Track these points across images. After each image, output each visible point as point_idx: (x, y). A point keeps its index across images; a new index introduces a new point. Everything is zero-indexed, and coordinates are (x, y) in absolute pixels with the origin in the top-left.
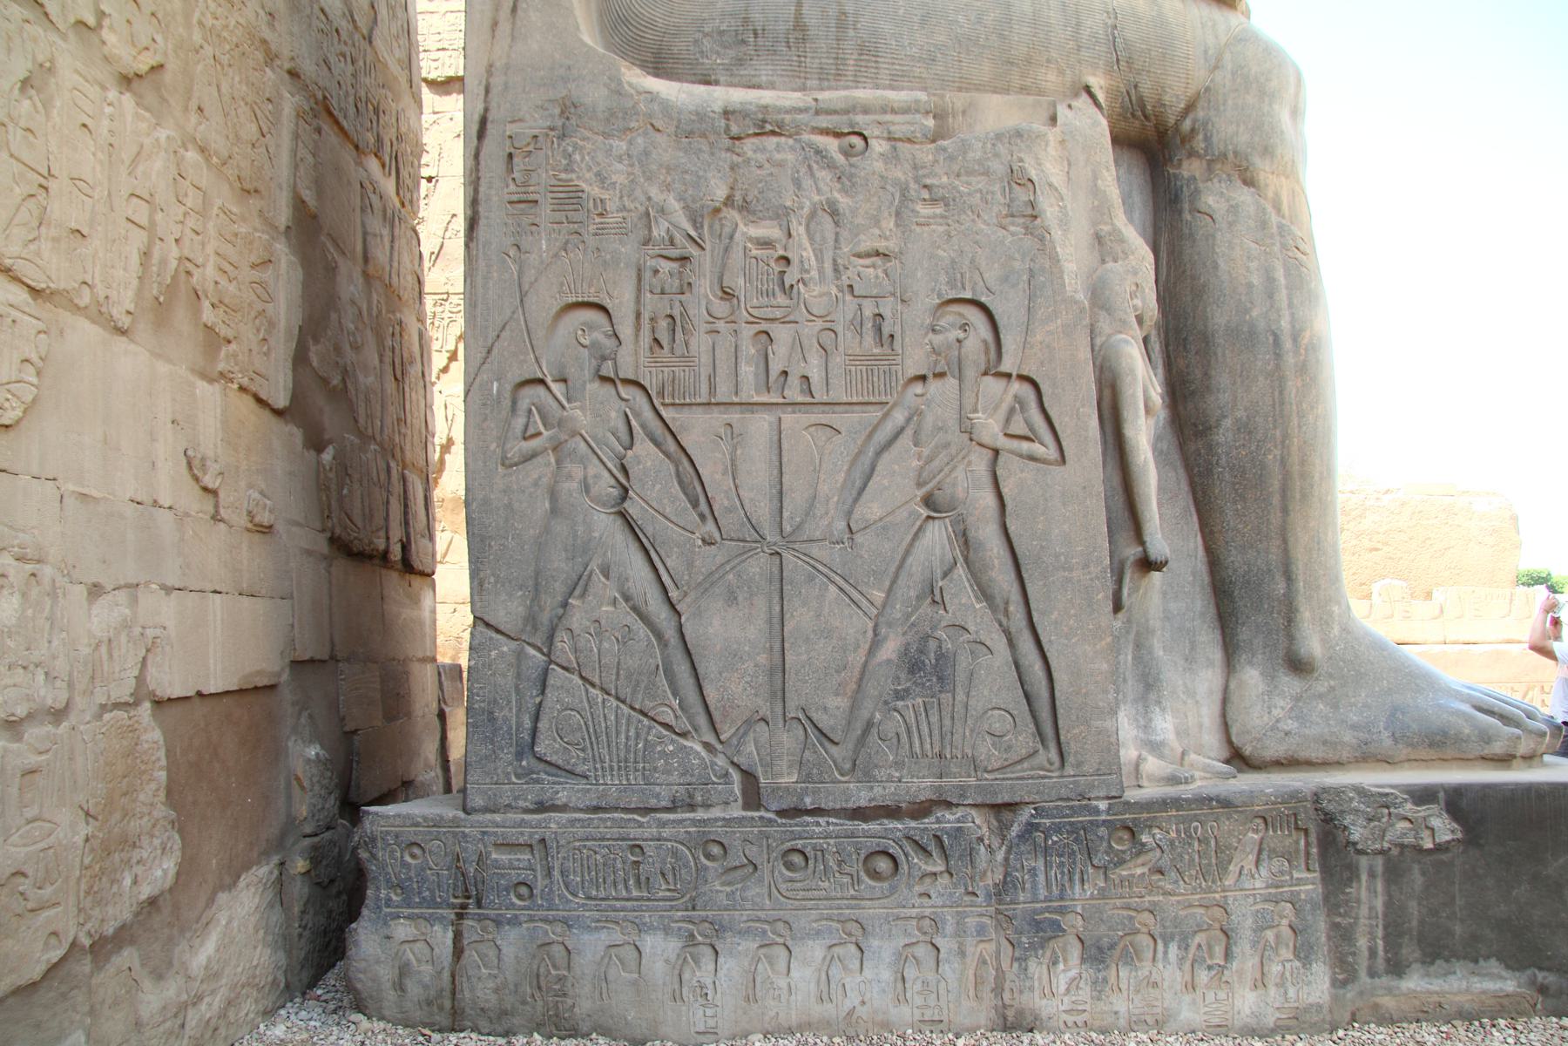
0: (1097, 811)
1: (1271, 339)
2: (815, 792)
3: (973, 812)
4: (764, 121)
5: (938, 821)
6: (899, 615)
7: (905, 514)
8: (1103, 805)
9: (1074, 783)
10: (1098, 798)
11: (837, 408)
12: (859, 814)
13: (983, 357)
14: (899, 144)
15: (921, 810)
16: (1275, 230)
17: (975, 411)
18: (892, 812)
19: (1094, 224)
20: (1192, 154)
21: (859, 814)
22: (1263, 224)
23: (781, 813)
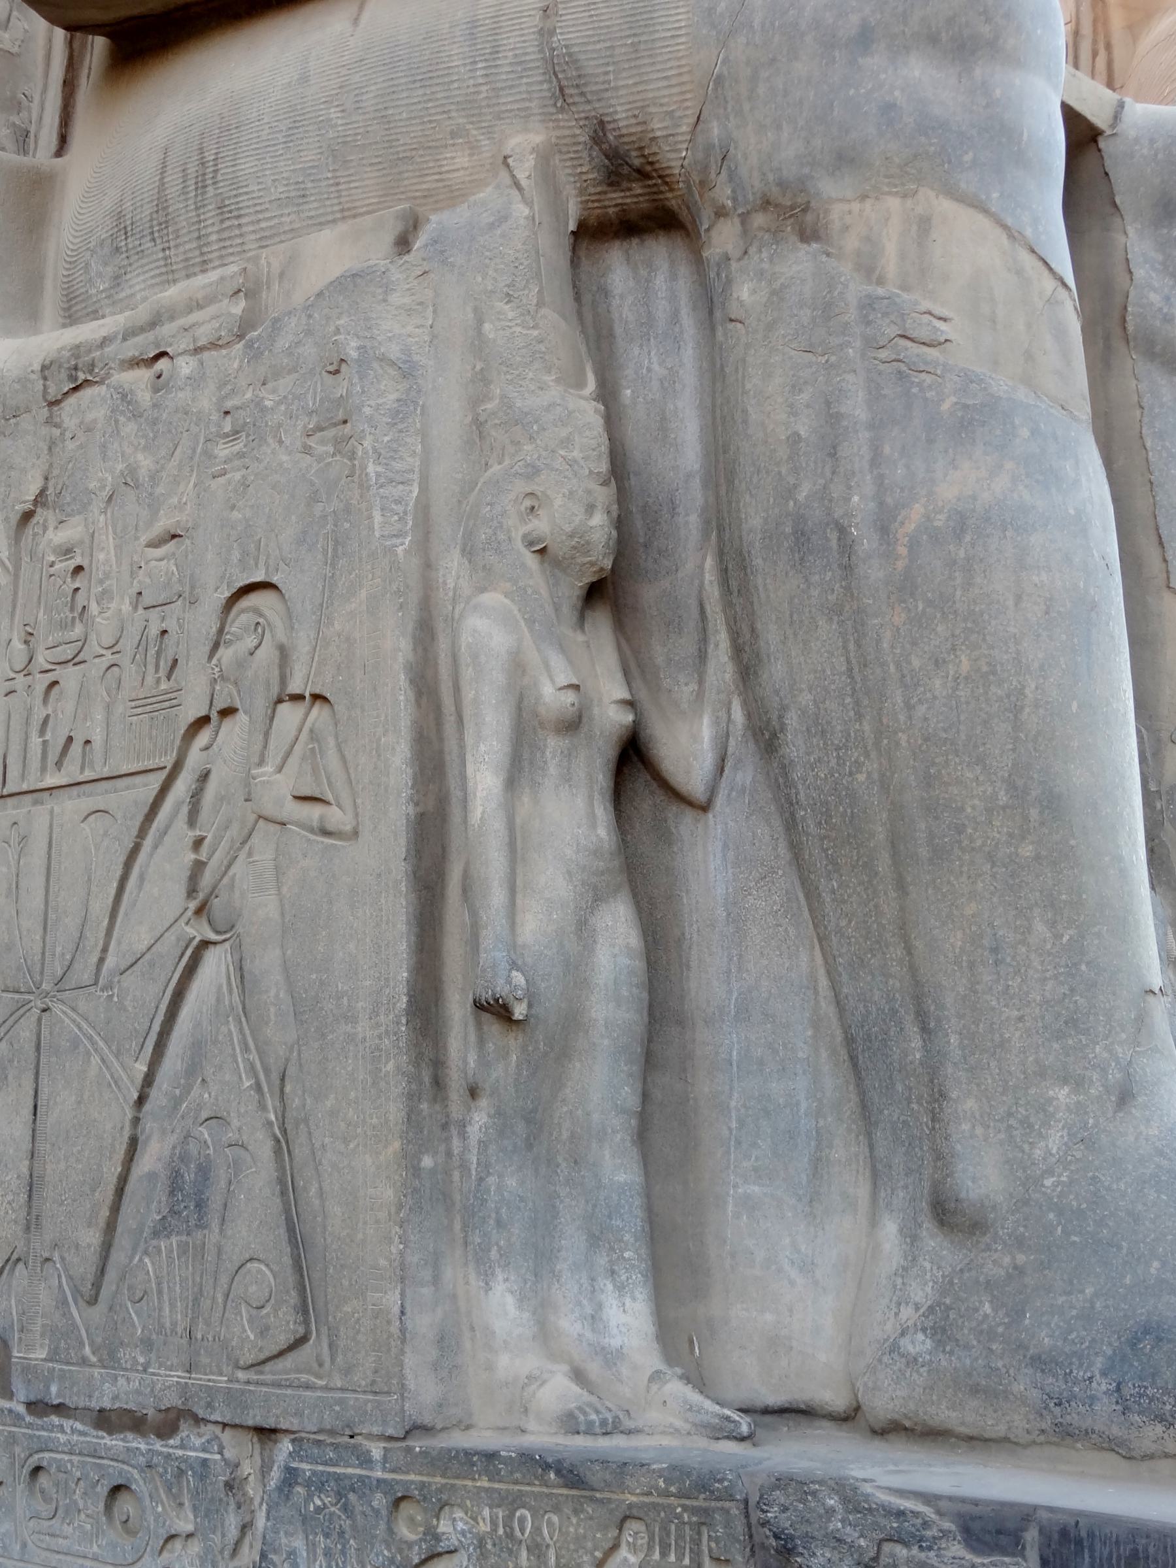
0: (366, 1461)
1: (833, 536)
2: (63, 1376)
3: (227, 1436)
4: (76, 368)
5: (182, 1446)
6: (164, 1102)
7: (173, 938)
8: (376, 1451)
9: (341, 1402)
10: (370, 1436)
11: (120, 783)
12: (105, 1420)
13: (277, 672)
14: (206, 355)
15: (168, 1424)
16: (852, 315)
17: (261, 762)
18: (135, 1423)
19: (475, 401)
20: (721, 213)
21: (105, 1420)
22: (827, 310)
23: (31, 1406)
